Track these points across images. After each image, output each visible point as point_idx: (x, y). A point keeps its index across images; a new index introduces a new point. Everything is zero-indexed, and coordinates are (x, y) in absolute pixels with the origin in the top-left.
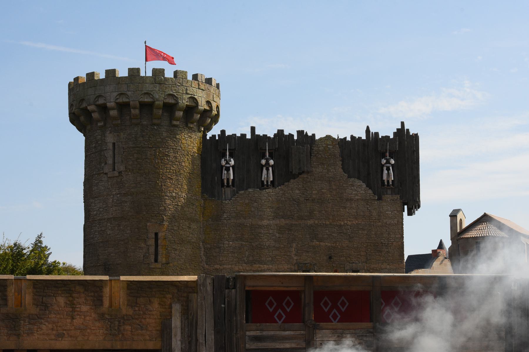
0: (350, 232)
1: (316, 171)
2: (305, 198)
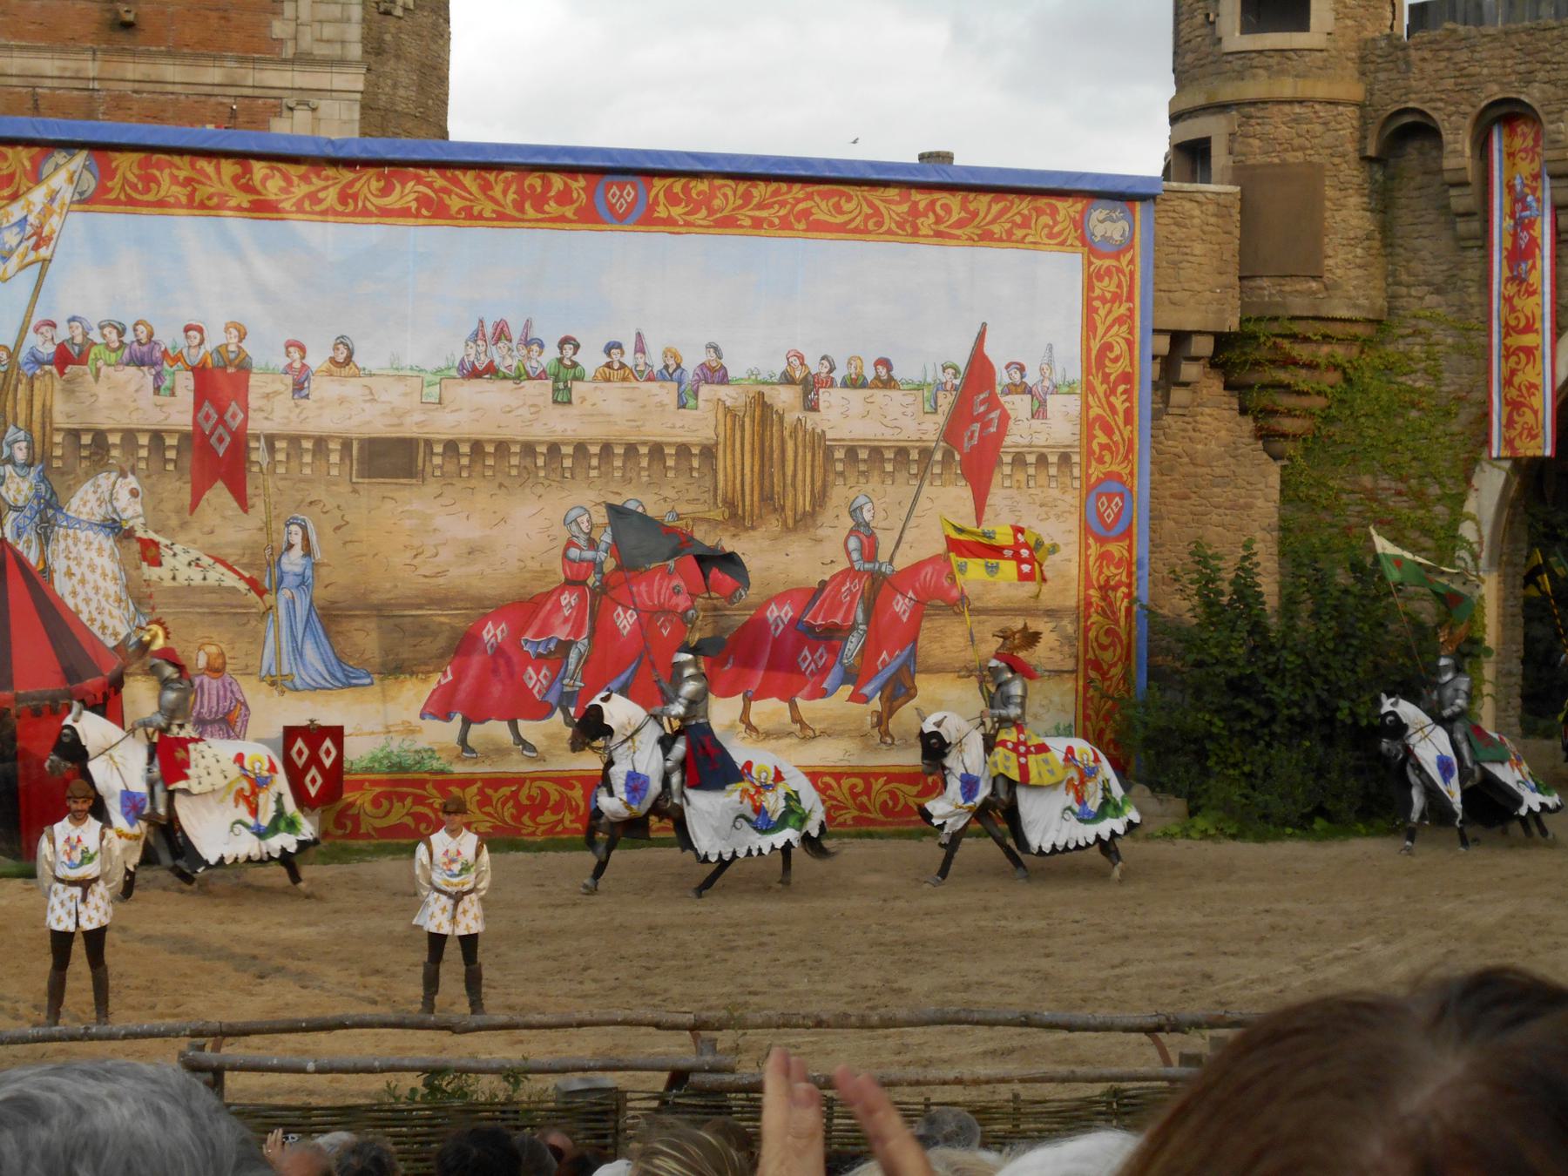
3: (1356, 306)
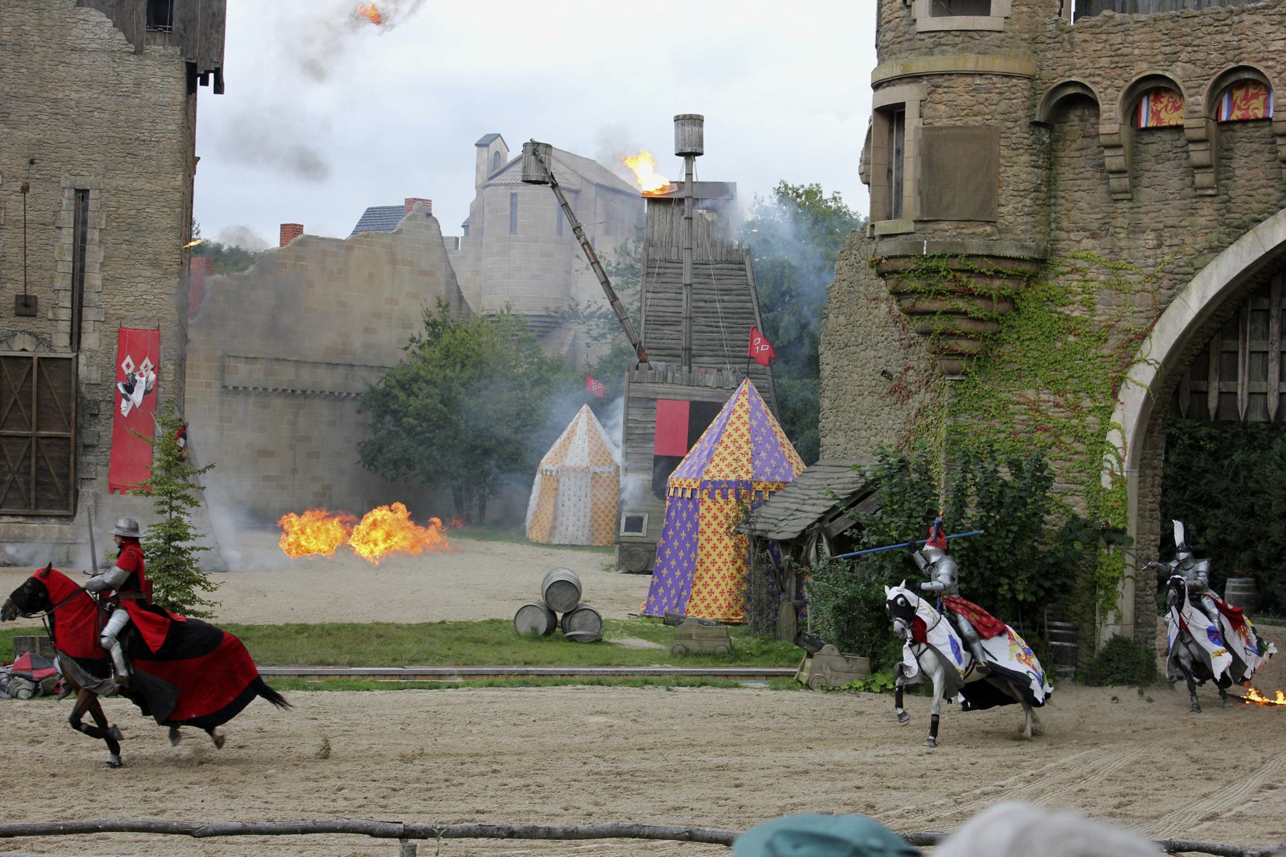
3: (1023, 247)
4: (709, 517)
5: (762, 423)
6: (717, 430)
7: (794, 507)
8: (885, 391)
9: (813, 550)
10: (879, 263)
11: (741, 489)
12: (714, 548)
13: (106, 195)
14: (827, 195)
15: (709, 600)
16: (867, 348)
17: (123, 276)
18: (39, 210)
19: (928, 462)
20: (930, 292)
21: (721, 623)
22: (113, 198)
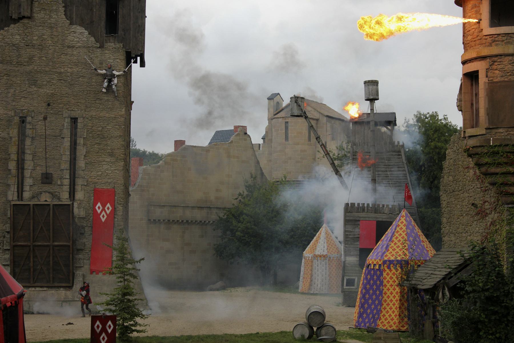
0: (70, 79)
1: (37, 17)
2: (25, 44)
4: (388, 278)
5: (412, 230)
6: (390, 235)
7: (431, 272)
8: (474, 213)
9: (441, 294)
10: (468, 150)
11: (403, 264)
12: (391, 293)
13: (86, 120)
14: (441, 117)
15: (389, 319)
16: (464, 192)
17: (95, 161)
18: (53, 129)
19: (497, 249)
20: (495, 163)
21: (396, 331)
22: (89, 121)
